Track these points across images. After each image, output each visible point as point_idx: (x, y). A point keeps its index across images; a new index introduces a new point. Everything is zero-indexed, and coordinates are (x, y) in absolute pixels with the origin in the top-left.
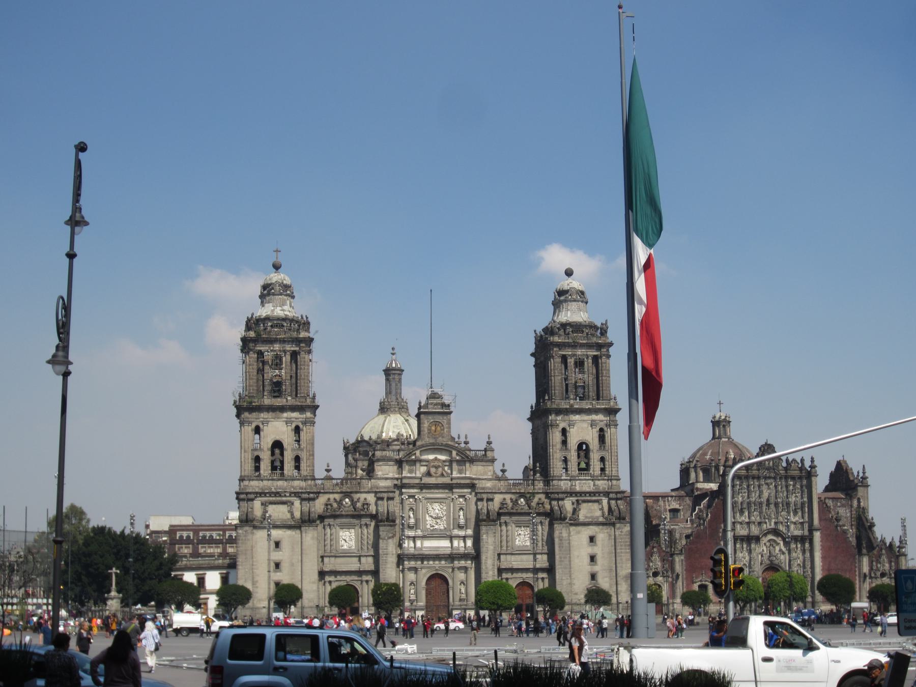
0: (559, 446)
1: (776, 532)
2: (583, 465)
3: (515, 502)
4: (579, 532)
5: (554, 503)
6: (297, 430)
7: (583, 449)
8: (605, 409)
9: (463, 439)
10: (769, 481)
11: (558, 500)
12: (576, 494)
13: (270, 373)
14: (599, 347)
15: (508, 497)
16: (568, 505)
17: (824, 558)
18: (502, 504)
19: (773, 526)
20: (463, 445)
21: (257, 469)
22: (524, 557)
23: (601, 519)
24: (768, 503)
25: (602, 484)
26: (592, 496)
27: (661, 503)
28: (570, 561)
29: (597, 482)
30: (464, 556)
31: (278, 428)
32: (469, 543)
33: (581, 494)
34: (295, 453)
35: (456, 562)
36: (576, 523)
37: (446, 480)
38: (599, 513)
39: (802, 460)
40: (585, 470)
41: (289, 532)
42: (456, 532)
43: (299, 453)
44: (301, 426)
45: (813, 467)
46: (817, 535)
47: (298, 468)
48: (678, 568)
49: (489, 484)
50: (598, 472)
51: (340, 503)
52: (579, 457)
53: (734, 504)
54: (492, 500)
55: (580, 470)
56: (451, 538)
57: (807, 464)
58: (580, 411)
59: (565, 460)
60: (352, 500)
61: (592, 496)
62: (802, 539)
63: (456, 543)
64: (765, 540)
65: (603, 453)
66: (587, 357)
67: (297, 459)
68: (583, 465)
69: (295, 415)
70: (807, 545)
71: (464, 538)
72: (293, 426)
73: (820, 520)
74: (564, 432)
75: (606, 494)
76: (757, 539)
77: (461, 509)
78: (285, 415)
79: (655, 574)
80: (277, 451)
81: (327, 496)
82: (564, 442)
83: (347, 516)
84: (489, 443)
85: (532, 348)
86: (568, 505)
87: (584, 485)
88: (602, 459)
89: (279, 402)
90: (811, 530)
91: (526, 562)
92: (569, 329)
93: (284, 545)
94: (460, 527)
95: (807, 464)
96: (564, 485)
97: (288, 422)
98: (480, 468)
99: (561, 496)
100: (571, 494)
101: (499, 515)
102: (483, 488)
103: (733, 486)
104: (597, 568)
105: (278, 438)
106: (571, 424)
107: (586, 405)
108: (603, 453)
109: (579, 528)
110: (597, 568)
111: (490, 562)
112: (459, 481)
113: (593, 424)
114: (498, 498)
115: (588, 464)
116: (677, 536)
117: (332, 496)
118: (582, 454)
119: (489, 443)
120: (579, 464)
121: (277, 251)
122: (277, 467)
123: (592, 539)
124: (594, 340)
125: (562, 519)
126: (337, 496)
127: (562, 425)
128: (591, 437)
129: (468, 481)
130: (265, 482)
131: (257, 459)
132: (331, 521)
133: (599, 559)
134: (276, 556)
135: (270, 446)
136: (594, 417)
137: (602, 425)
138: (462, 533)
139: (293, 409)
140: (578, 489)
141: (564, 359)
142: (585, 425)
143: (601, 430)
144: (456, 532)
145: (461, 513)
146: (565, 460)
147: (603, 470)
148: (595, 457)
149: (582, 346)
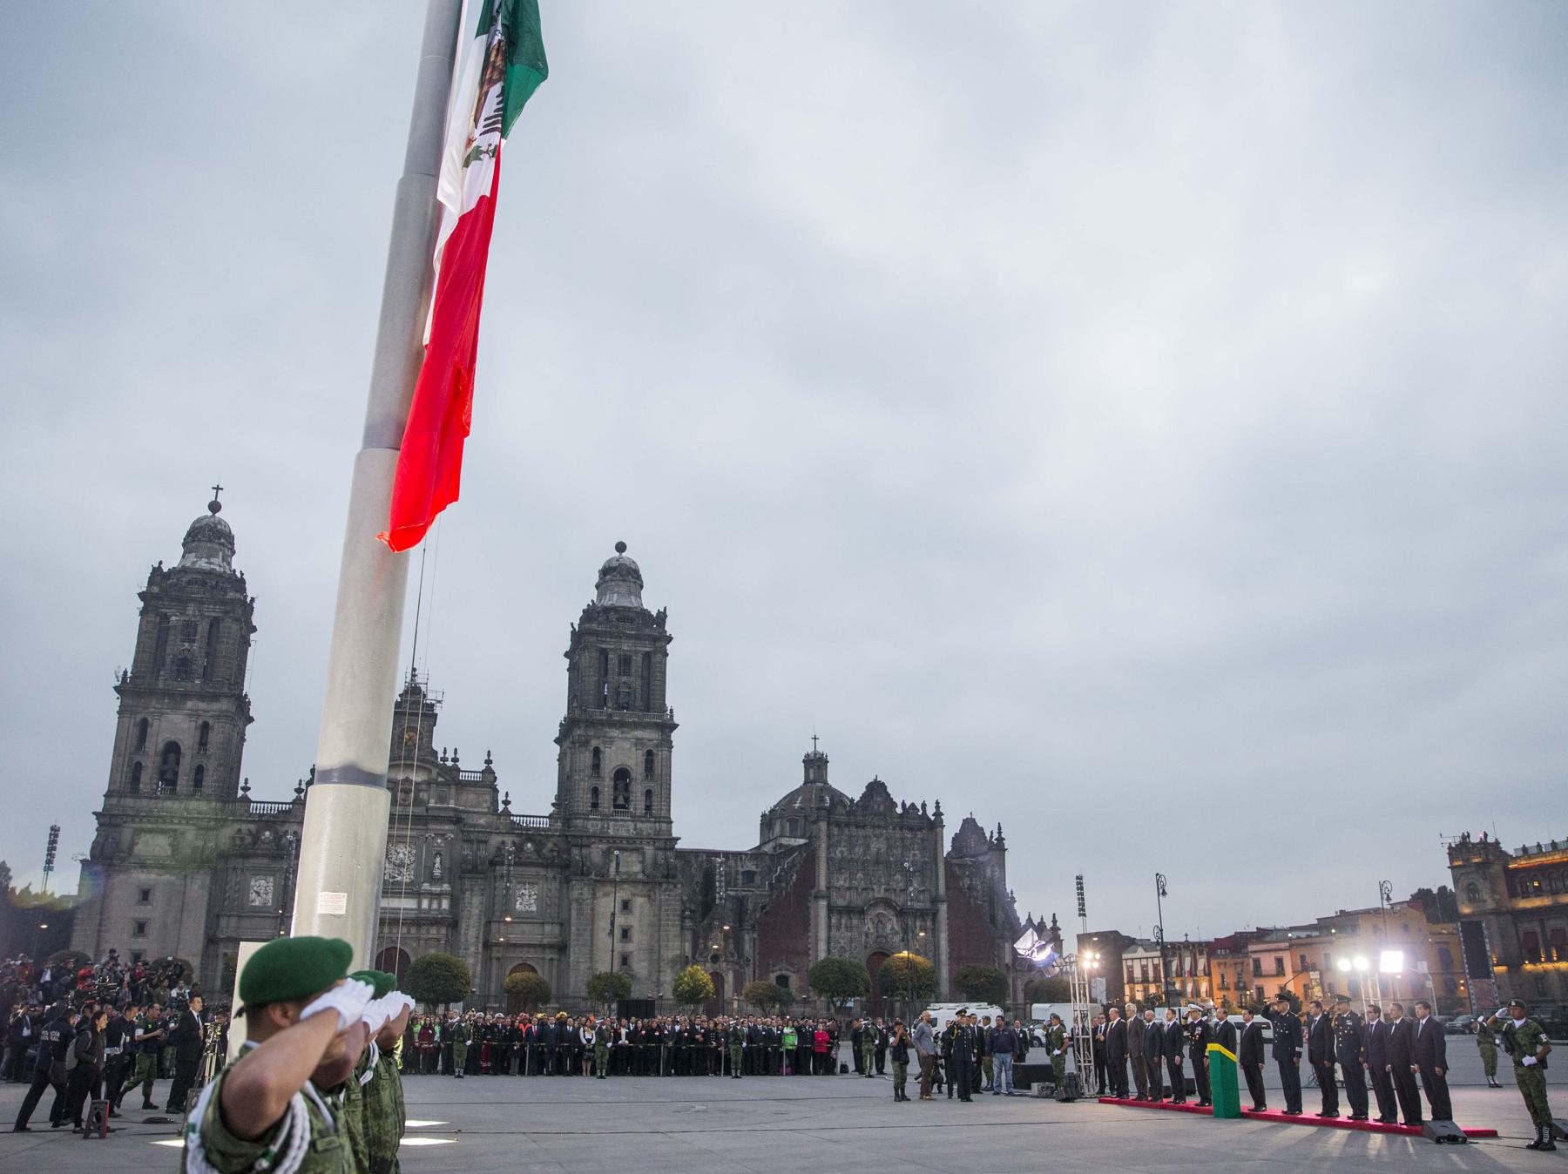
0: (588, 772)
1: (887, 903)
2: (621, 801)
3: (519, 848)
4: (606, 895)
5: (575, 851)
6: (205, 727)
7: (622, 775)
8: (657, 725)
9: (450, 755)
10: (878, 831)
11: (581, 846)
12: (608, 839)
13: (176, 646)
14: (655, 639)
15: (509, 840)
16: (596, 852)
17: (950, 941)
18: (499, 849)
19: (882, 894)
20: (449, 763)
21: (136, 779)
22: (526, 928)
23: (640, 876)
24: (877, 863)
25: (646, 827)
26: (632, 844)
27: (732, 862)
28: (592, 935)
29: (639, 825)
30: (436, 922)
31: (176, 725)
32: (445, 904)
33: (615, 839)
34: (197, 762)
35: (424, 930)
36: (603, 879)
37: (421, 811)
38: (637, 868)
39: (924, 805)
40: (621, 806)
41: (166, 877)
42: (426, 886)
43: (204, 762)
44: (211, 722)
45: (938, 814)
46: (943, 908)
47: (198, 783)
48: (748, 948)
49: (482, 821)
50: (641, 810)
51: (256, 837)
52: (616, 788)
53: (829, 859)
54: (486, 842)
55: (616, 806)
56: (418, 895)
57: (930, 811)
58: (622, 725)
59: (595, 791)
60: (275, 833)
61: (632, 844)
62: (922, 914)
63: (425, 904)
64: (873, 913)
65: (652, 785)
66: (636, 652)
67: (200, 770)
68: (621, 801)
69: (202, 705)
70: (929, 923)
71: (439, 896)
72: (200, 722)
73: (947, 887)
74: (597, 752)
75: (652, 840)
76: (861, 912)
77: (439, 853)
78: (190, 704)
79: (715, 959)
80: (172, 757)
81: (236, 826)
82: (596, 767)
83: (264, 856)
84: (489, 762)
85: (567, 645)
86: (596, 852)
87: (623, 828)
88: (649, 793)
89: (182, 686)
90: (935, 901)
91: (529, 934)
92: (612, 616)
93: (158, 897)
94: (433, 880)
95: (930, 811)
96: (593, 826)
97: (194, 714)
98: (471, 796)
99: (585, 841)
100: (602, 837)
101: (493, 864)
102: (474, 826)
103: (829, 837)
104: (631, 947)
105: (173, 738)
106: (611, 741)
107: (628, 716)
108: (652, 785)
109: (609, 888)
110: (631, 947)
111: (472, 932)
112: (436, 813)
113: (638, 742)
114: (495, 840)
115: (627, 800)
116: (750, 906)
117: (244, 827)
118: (621, 785)
119: (489, 762)
120: (615, 799)
121: (218, 488)
122: (168, 777)
123: (626, 906)
124: (647, 631)
125: (583, 873)
126: (253, 827)
127: (594, 743)
128: (634, 761)
129: (451, 814)
130: (144, 802)
131: (138, 767)
132: (239, 863)
133: (636, 936)
134: (143, 912)
135: (161, 747)
136: (638, 733)
137: (650, 745)
138: (436, 889)
139: (202, 696)
140: (611, 832)
141: (604, 653)
142: (627, 745)
143: (650, 753)
144: (426, 886)
145: (438, 860)
146: (595, 791)
147: (648, 808)
148: (638, 790)
149: (629, 637)
